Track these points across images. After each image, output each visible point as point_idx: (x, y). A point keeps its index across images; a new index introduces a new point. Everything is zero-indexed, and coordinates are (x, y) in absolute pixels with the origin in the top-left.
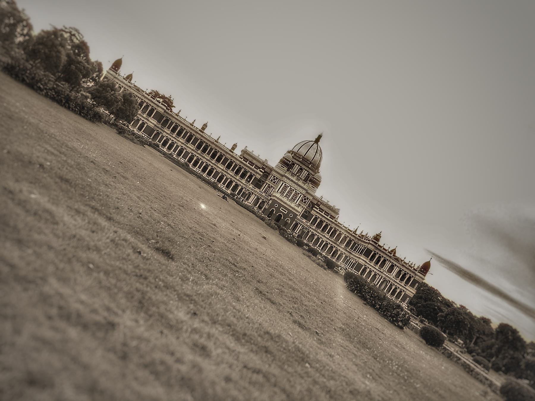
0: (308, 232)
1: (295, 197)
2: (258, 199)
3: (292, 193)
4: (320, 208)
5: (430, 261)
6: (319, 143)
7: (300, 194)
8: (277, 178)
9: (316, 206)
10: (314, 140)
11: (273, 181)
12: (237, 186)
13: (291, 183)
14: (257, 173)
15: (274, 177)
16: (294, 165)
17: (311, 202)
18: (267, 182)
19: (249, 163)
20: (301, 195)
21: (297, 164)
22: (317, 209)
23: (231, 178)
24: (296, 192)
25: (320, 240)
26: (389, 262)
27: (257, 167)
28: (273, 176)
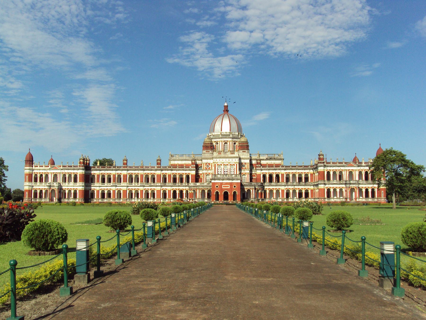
0: (265, 192)
2: (203, 191)
5: (380, 148)
8: (209, 164)
12: (181, 192)
15: (206, 164)
16: (217, 143)
20: (237, 165)
22: (260, 167)
23: (172, 188)
25: (280, 191)
26: (346, 172)
27: (187, 166)
28: (205, 164)
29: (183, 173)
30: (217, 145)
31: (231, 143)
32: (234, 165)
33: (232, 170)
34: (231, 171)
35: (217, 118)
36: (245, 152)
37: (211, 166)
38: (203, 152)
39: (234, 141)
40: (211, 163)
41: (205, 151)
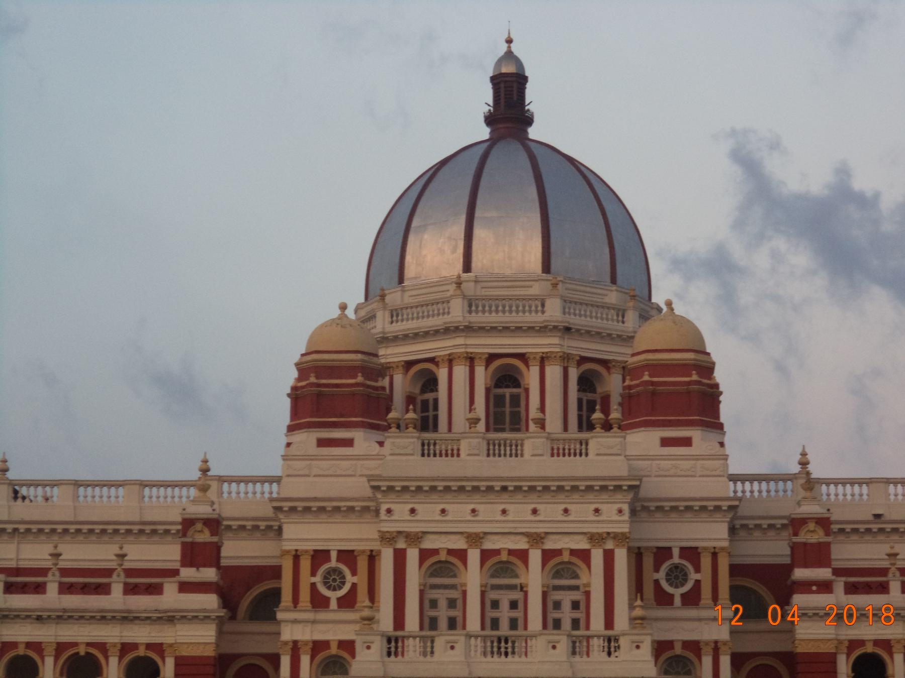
1: (575, 605)
3: (522, 588)
4: (837, 572)
6: (534, 133)
7: (597, 557)
8: (348, 557)
9: (800, 574)
10: (484, 133)
11: (333, 596)
13: (459, 510)
14: (170, 618)
15: (320, 557)
16: (431, 383)
17: (735, 570)
18: (288, 633)
19: (66, 589)
20: (609, 557)
21: (451, 361)
22: (825, 587)
24: (548, 555)
28: (305, 564)
29: (102, 647)
30: (430, 396)
31: (554, 372)
32: (584, 556)
33: (567, 606)
34: (553, 615)
35: (430, 173)
36: (686, 442)
37: (361, 579)
38: (293, 450)
39: (583, 360)
40: (367, 546)
41: (307, 439)
